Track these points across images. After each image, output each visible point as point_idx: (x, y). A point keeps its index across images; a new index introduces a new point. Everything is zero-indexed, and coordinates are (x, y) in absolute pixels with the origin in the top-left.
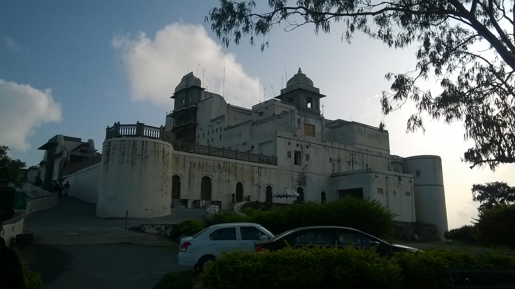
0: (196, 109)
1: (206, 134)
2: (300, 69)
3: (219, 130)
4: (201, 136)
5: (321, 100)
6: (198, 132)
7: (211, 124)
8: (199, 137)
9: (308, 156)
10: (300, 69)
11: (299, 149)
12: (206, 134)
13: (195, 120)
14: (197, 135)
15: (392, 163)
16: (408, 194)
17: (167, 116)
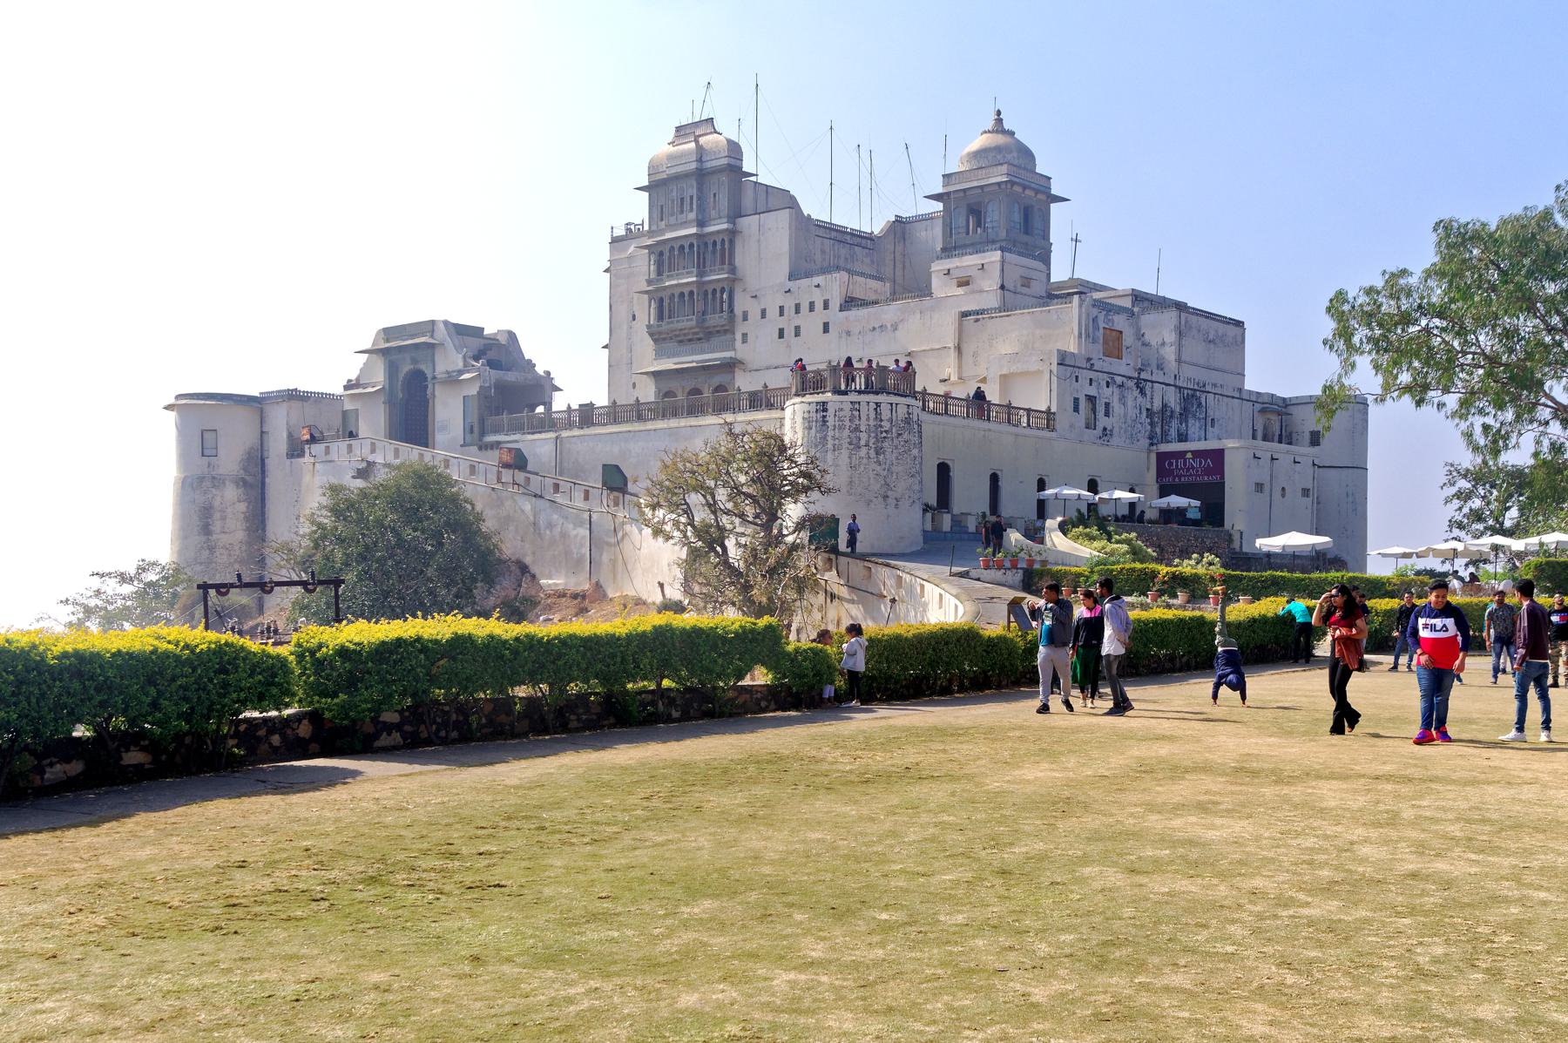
0: (733, 233)
1: (773, 312)
2: (999, 113)
3: (819, 305)
4: (754, 314)
5: (1055, 208)
6: (742, 303)
7: (791, 285)
8: (745, 318)
9: (1107, 405)
10: (999, 113)
11: (1092, 391)
12: (773, 312)
13: (733, 270)
14: (738, 311)
15: (1263, 411)
16: (1306, 492)
17: (615, 241)
